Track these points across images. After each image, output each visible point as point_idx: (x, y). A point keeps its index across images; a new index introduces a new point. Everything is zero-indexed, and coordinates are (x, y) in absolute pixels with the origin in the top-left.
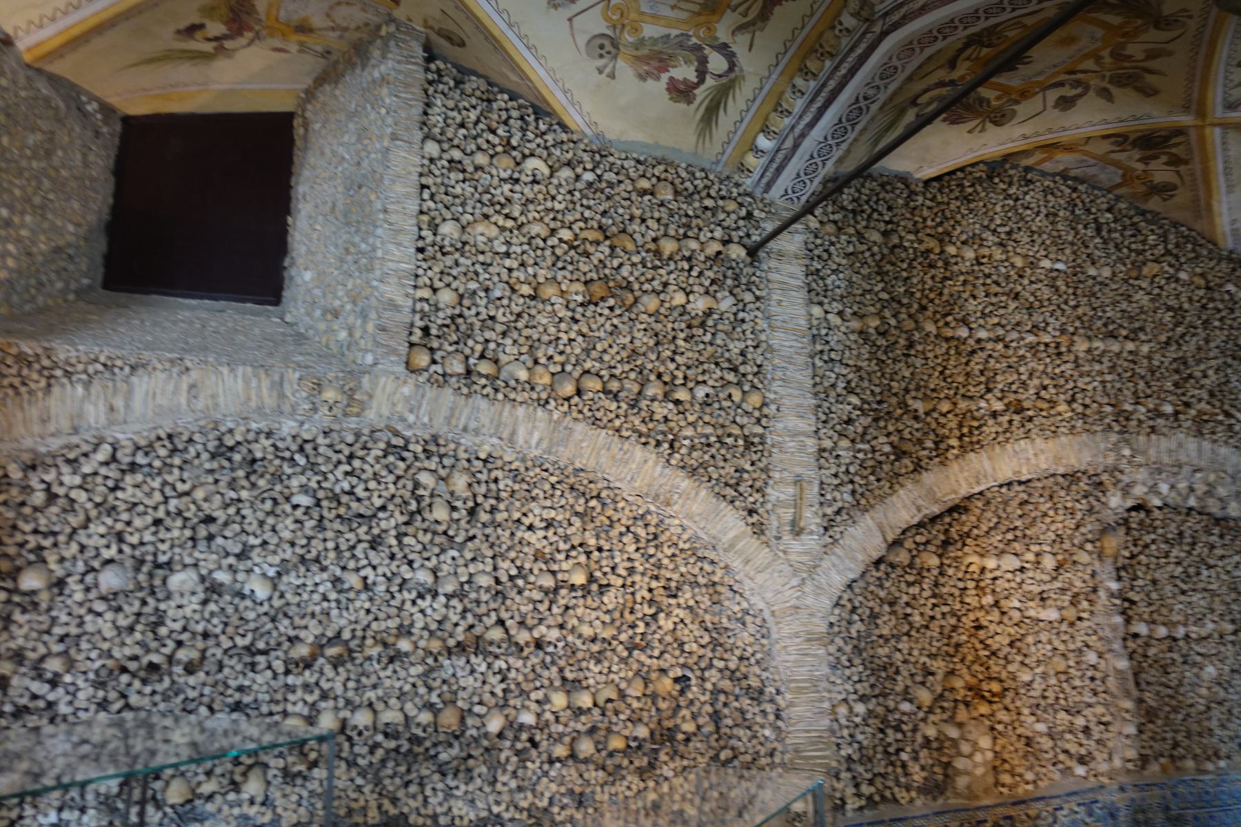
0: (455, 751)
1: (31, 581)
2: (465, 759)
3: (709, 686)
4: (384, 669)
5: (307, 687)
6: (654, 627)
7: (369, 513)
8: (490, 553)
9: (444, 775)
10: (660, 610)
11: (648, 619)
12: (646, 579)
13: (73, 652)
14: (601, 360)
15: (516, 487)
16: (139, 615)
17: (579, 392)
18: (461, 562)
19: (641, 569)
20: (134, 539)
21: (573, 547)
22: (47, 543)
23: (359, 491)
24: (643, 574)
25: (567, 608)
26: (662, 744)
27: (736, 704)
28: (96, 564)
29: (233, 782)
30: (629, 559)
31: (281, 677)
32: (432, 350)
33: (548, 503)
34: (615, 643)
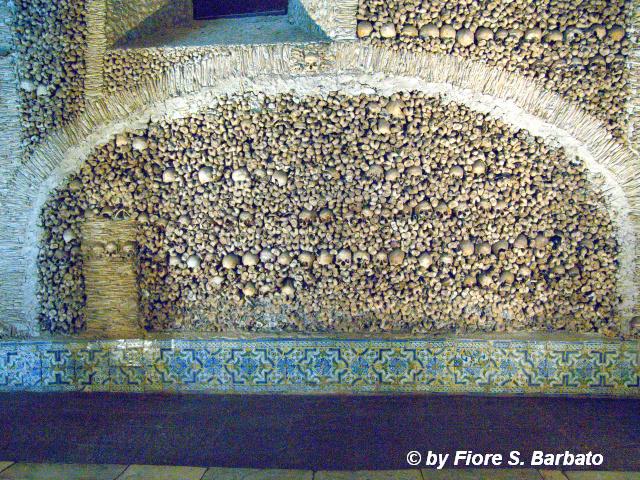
0: (402, 276)
1: (167, 177)
2: (407, 283)
3: (575, 244)
4: (356, 227)
5: (311, 236)
6: (534, 202)
7: (339, 131)
8: (416, 154)
9: (396, 291)
10: (537, 192)
11: (530, 197)
12: (528, 171)
13: (190, 213)
14: (491, 16)
15: (434, 110)
16: (220, 194)
17: (476, 42)
18: (400, 160)
19: (525, 163)
20: (213, 154)
21: (475, 149)
22: (173, 157)
23: (332, 117)
24: (526, 167)
25: (472, 190)
26: (539, 280)
27: (595, 257)
28: (196, 167)
29: (277, 287)
30: (516, 157)
31: (296, 230)
32: (373, 23)
33: (456, 120)
34: (506, 213)
